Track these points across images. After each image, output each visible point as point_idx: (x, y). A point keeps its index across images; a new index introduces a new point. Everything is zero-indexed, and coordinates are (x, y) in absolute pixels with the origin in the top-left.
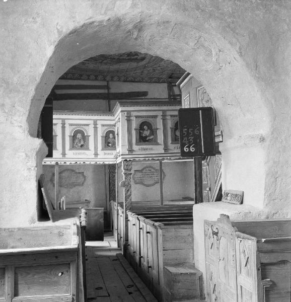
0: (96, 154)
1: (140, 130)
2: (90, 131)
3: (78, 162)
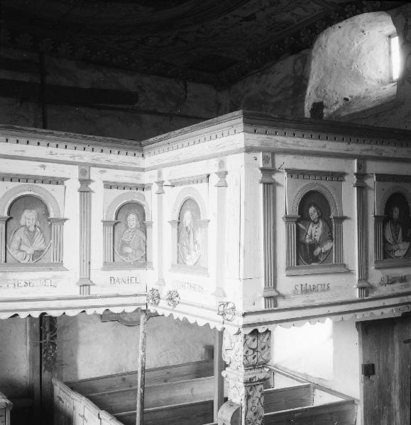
0: (85, 285)
1: (298, 221)
2: (66, 202)
3: (23, 315)
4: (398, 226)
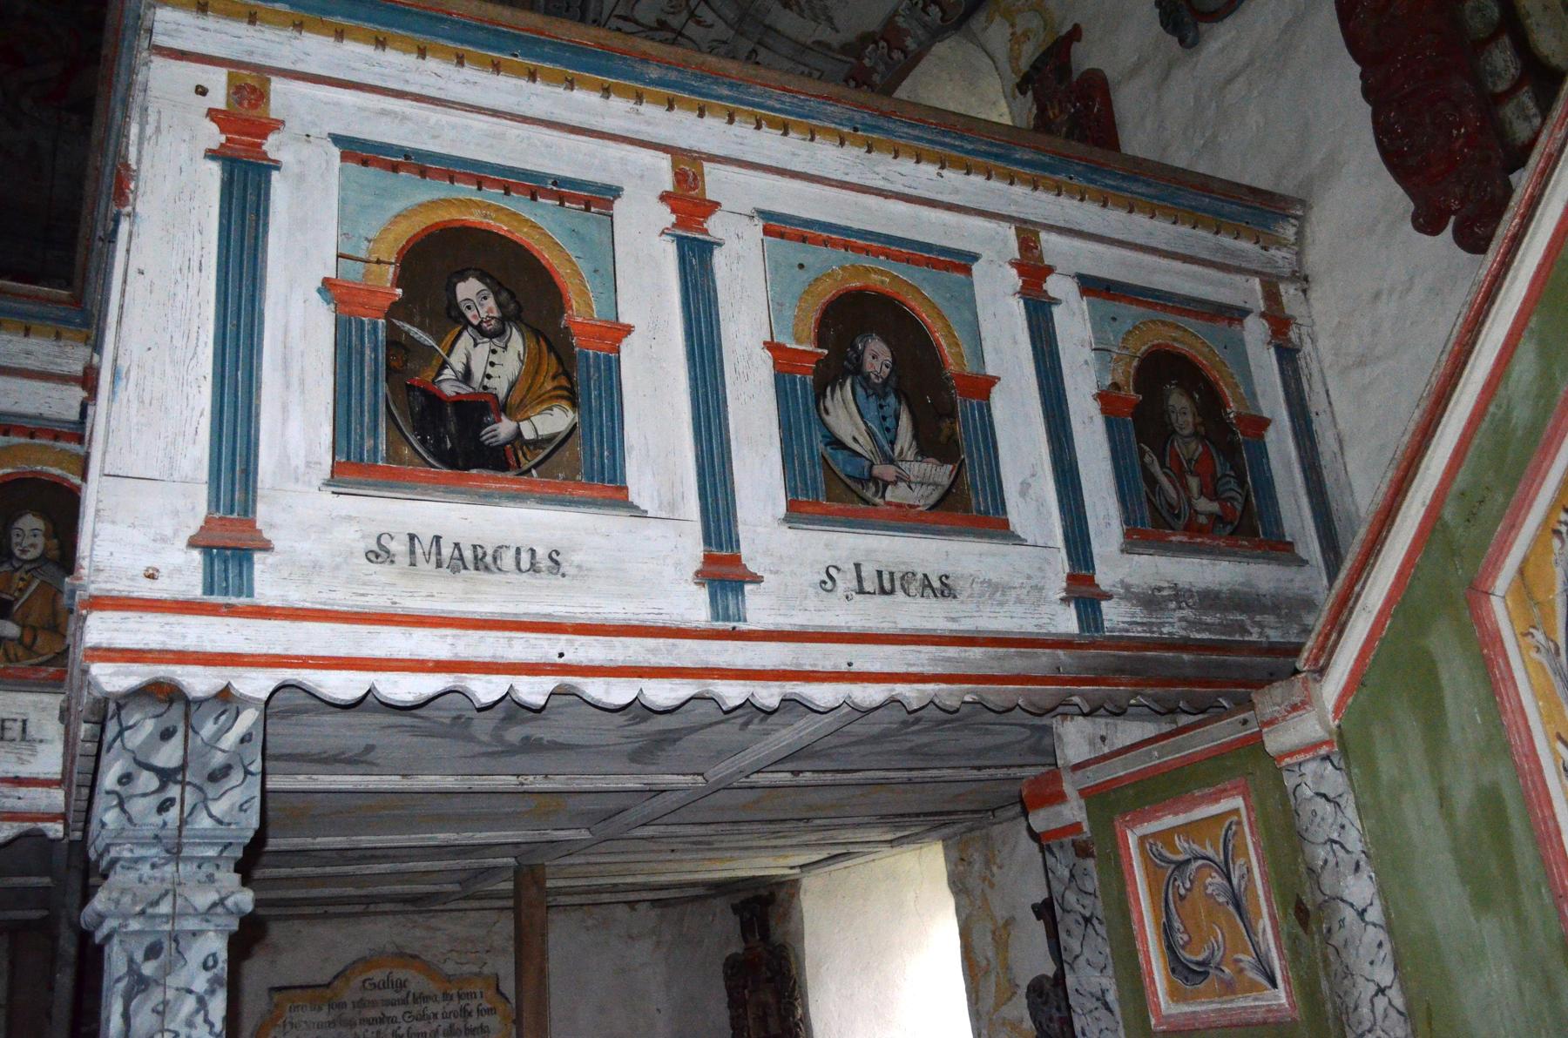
4: (892, 400)
